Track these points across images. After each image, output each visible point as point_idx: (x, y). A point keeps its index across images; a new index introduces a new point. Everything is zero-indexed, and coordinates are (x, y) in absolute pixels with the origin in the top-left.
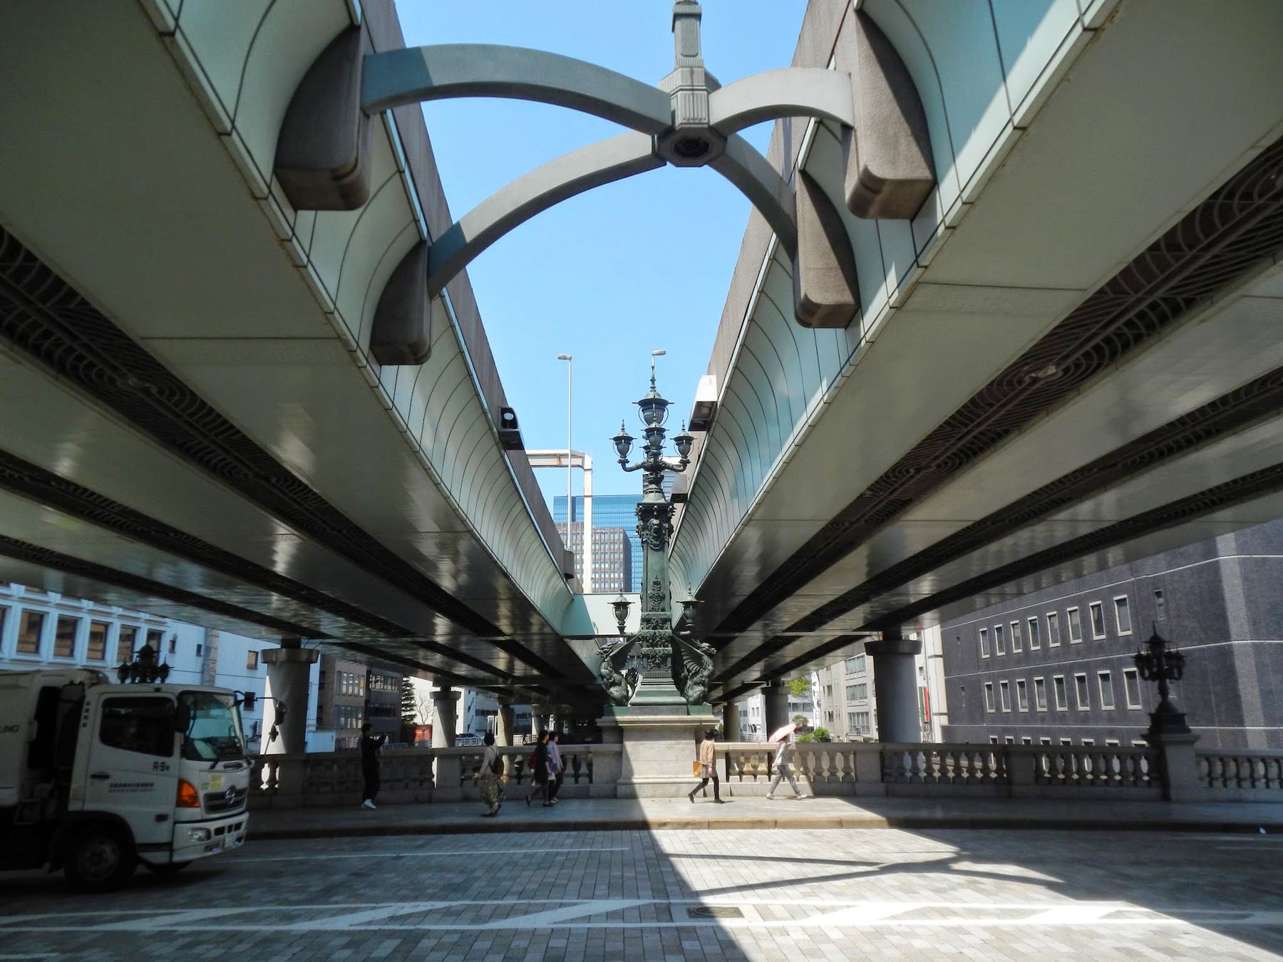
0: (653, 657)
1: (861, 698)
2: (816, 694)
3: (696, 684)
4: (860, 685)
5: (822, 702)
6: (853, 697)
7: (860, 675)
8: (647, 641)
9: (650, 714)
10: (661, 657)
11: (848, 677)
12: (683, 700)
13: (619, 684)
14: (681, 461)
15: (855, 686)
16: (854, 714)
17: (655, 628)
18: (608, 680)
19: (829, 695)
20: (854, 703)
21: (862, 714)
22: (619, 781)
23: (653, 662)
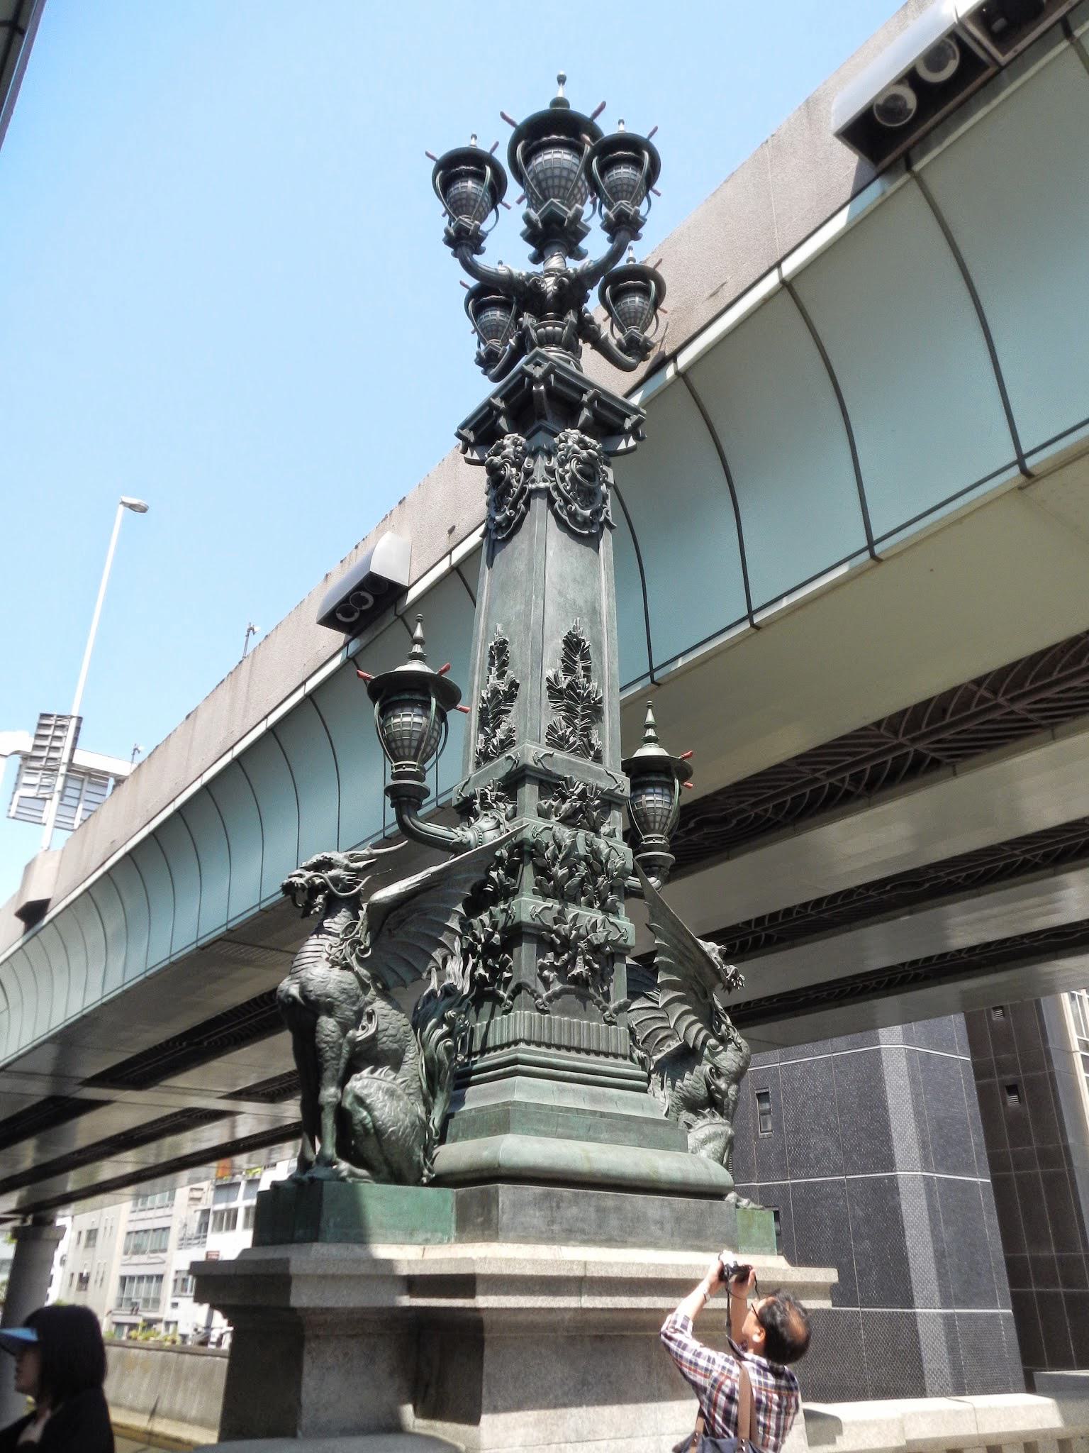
0: (567, 944)
1: (154, 1251)
4: (155, 1230)
6: (138, 1250)
7: (160, 1212)
8: (542, 870)
9: (589, 1240)
10: (596, 949)
11: (134, 1216)
13: (394, 1060)
15: (146, 1231)
16: (132, 1278)
17: (567, 820)
18: (345, 1027)
19: (87, 1246)
20: (136, 1259)
21: (150, 1278)
23: (562, 971)
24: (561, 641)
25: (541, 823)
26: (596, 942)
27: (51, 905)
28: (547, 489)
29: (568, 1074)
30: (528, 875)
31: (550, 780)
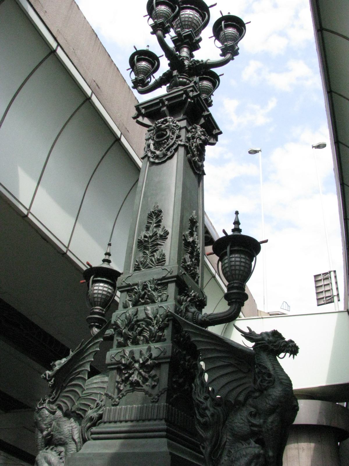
3: (244, 438)
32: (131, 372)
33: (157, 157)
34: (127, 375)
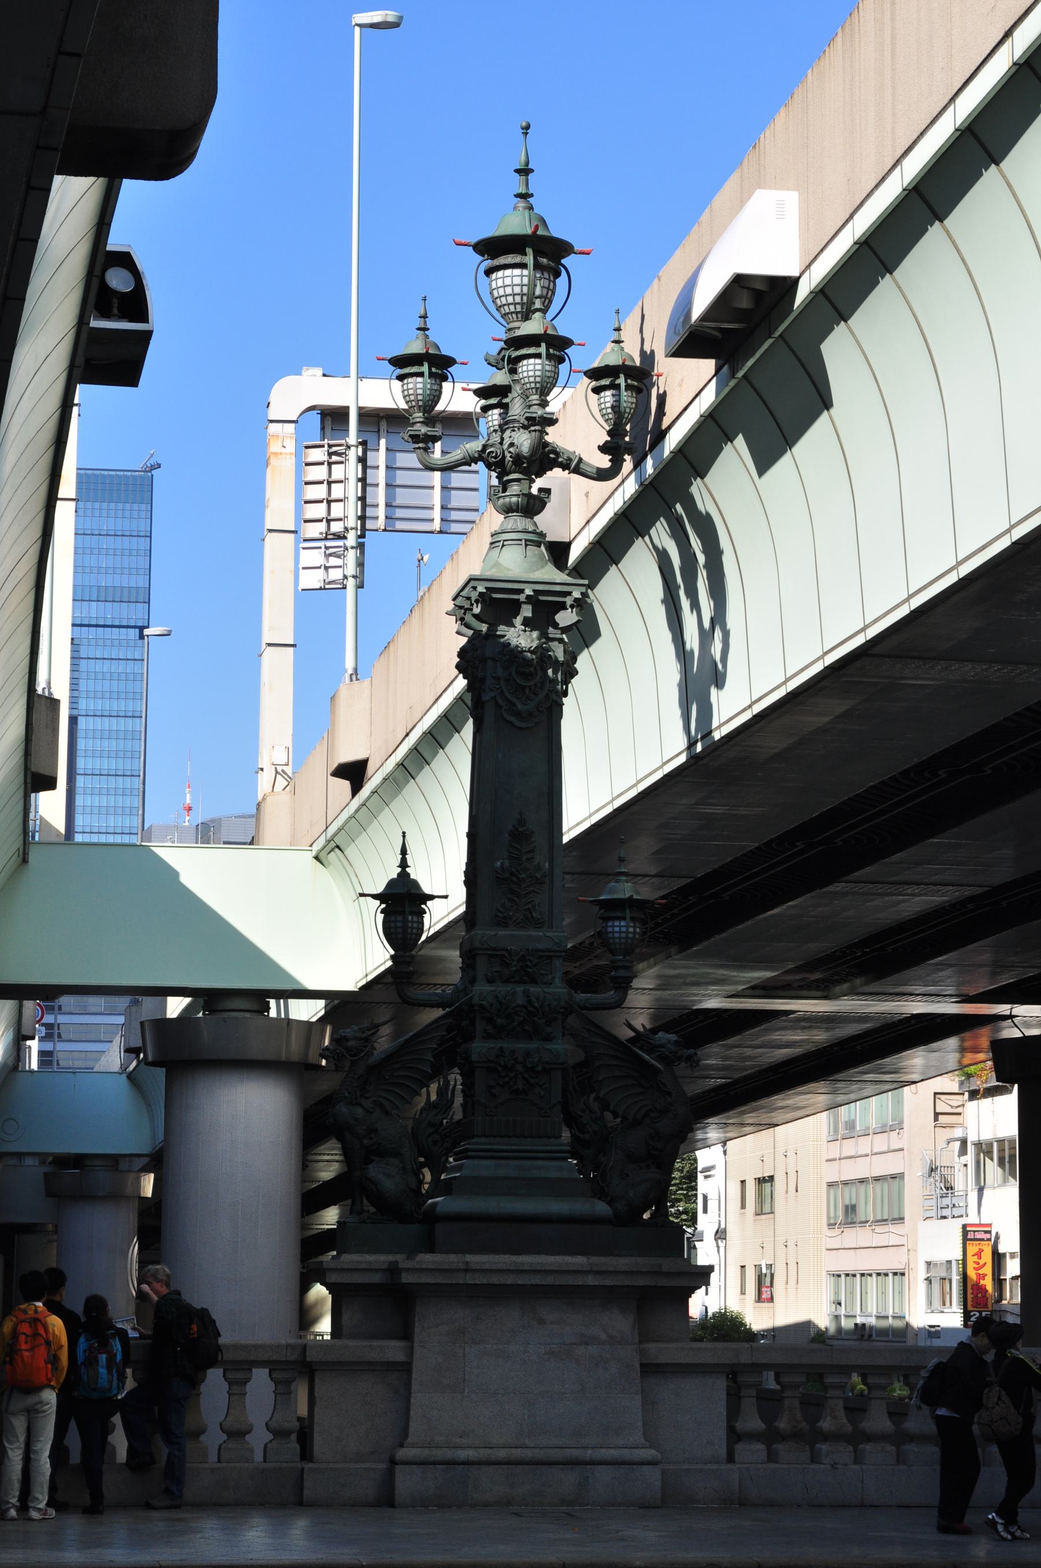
2: (712, 1205)
4: (877, 1179)
5: (732, 1232)
6: (850, 1216)
7: (880, 1142)
11: (834, 1150)
12: (601, 1208)
14: (604, 449)
15: (862, 1181)
19: (760, 1213)
22: (402, 1454)
24: (507, 835)
25: (489, 988)
26: (529, 1066)
27: (371, 768)
28: (494, 698)
29: (506, 1154)
30: (480, 1026)
31: (497, 953)
32: (511, 1075)
33: (518, 714)
34: (507, 1079)
